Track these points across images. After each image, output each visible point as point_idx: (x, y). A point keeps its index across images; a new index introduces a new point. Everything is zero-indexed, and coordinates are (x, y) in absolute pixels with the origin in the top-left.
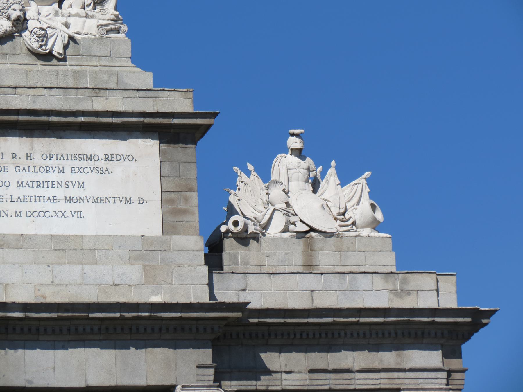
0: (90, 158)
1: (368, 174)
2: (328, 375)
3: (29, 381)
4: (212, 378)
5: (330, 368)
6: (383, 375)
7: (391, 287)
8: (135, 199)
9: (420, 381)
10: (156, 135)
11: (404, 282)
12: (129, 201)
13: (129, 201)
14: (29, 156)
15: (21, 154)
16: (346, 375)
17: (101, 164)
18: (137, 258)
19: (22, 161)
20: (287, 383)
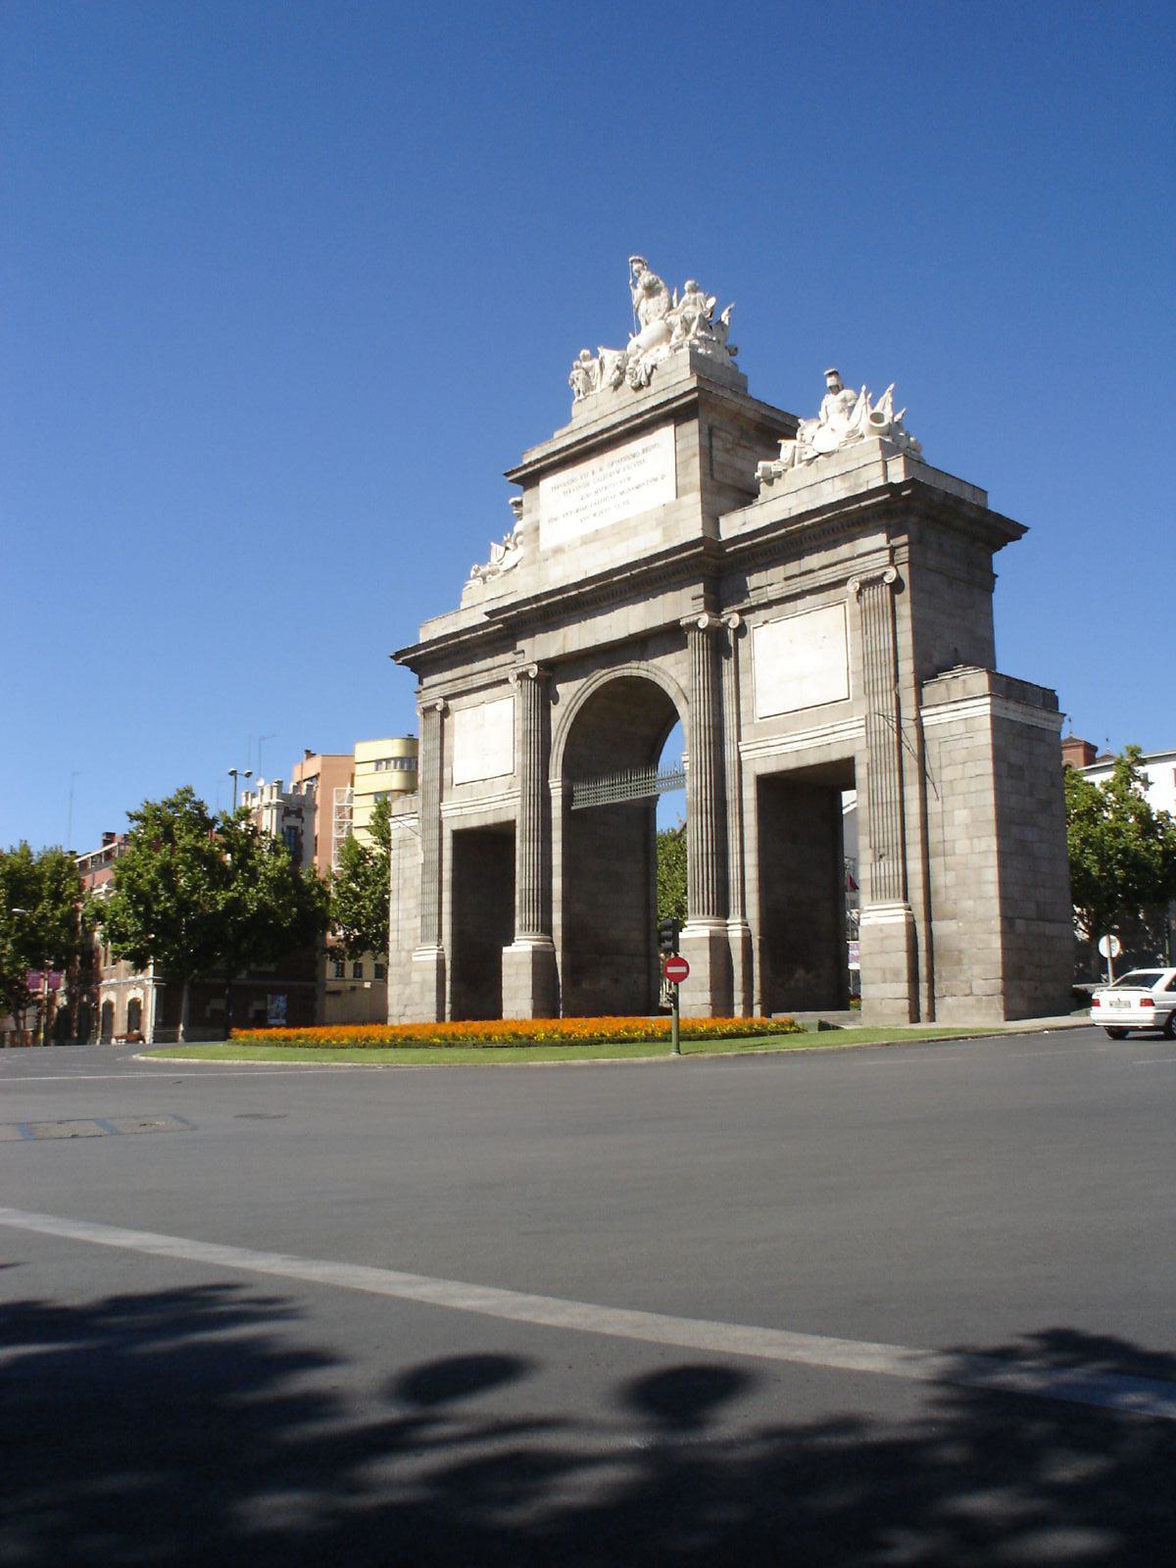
0: (634, 456)
1: (892, 386)
2: (798, 579)
3: (598, 640)
4: (702, 606)
5: (803, 570)
6: (839, 567)
7: (847, 485)
8: (659, 478)
9: (867, 564)
10: (673, 420)
11: (858, 476)
12: (656, 480)
13: (656, 480)
14: (601, 470)
15: (597, 470)
16: (811, 576)
17: (640, 458)
18: (658, 525)
19: (599, 474)
20: (772, 594)
